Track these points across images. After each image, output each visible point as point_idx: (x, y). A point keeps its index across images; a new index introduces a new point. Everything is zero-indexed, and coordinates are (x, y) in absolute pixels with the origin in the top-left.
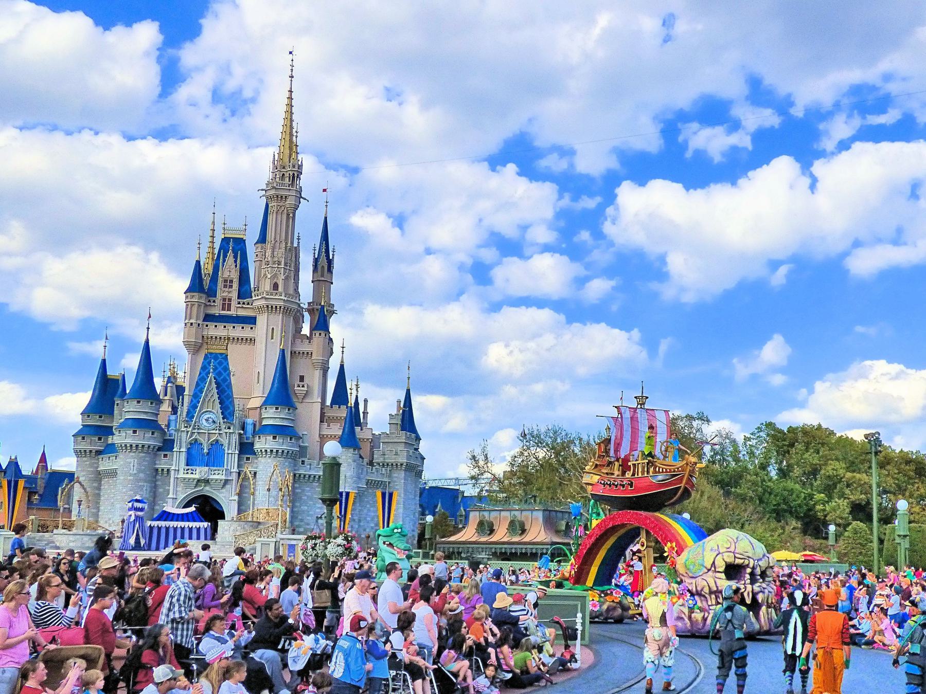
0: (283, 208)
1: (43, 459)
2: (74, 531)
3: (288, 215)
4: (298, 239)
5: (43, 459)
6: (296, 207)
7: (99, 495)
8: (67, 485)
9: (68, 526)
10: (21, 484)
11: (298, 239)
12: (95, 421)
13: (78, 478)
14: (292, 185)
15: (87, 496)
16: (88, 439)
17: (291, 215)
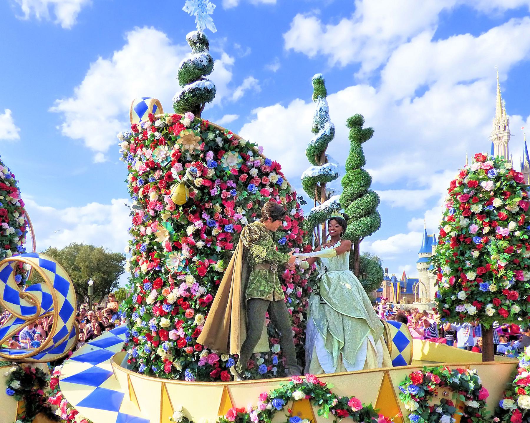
0: (501, 143)
1: (404, 274)
2: (422, 303)
3: (504, 145)
4: (511, 156)
5: (404, 274)
6: (508, 141)
7: (429, 287)
8: (416, 284)
9: (419, 300)
10: (398, 284)
11: (511, 156)
12: (424, 255)
13: (421, 280)
14: (505, 130)
15: (426, 288)
16: (422, 264)
17: (506, 145)
